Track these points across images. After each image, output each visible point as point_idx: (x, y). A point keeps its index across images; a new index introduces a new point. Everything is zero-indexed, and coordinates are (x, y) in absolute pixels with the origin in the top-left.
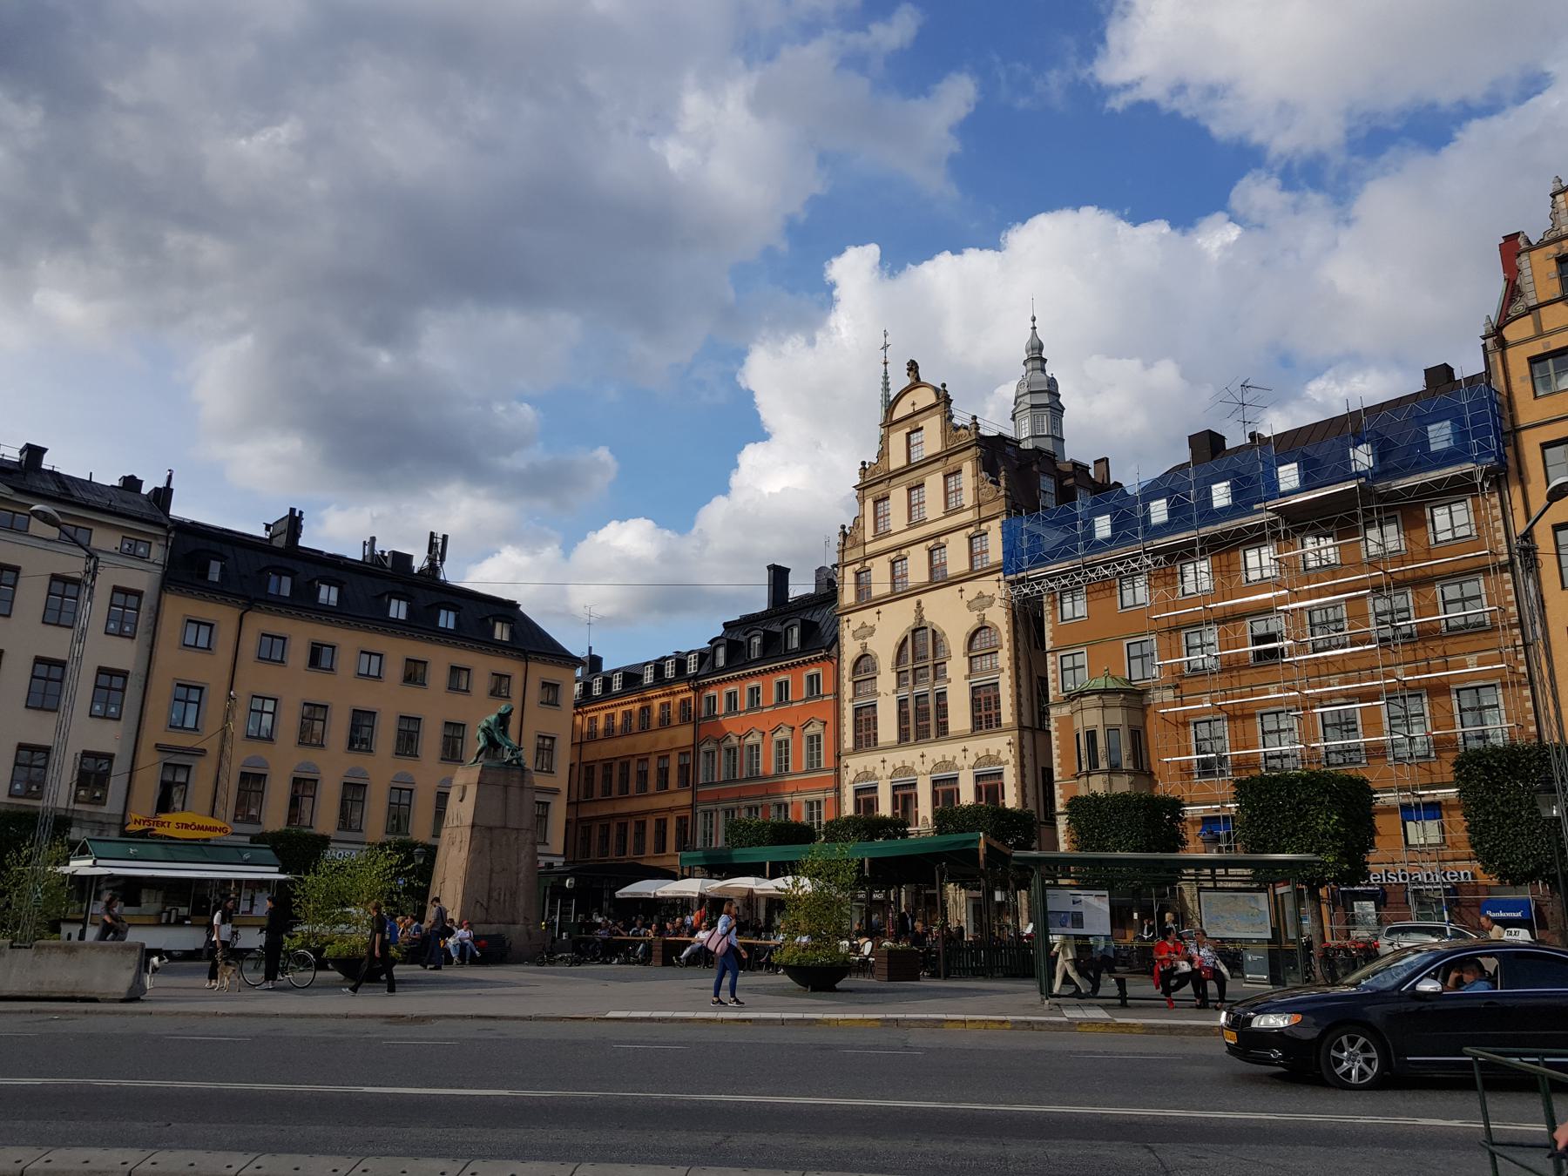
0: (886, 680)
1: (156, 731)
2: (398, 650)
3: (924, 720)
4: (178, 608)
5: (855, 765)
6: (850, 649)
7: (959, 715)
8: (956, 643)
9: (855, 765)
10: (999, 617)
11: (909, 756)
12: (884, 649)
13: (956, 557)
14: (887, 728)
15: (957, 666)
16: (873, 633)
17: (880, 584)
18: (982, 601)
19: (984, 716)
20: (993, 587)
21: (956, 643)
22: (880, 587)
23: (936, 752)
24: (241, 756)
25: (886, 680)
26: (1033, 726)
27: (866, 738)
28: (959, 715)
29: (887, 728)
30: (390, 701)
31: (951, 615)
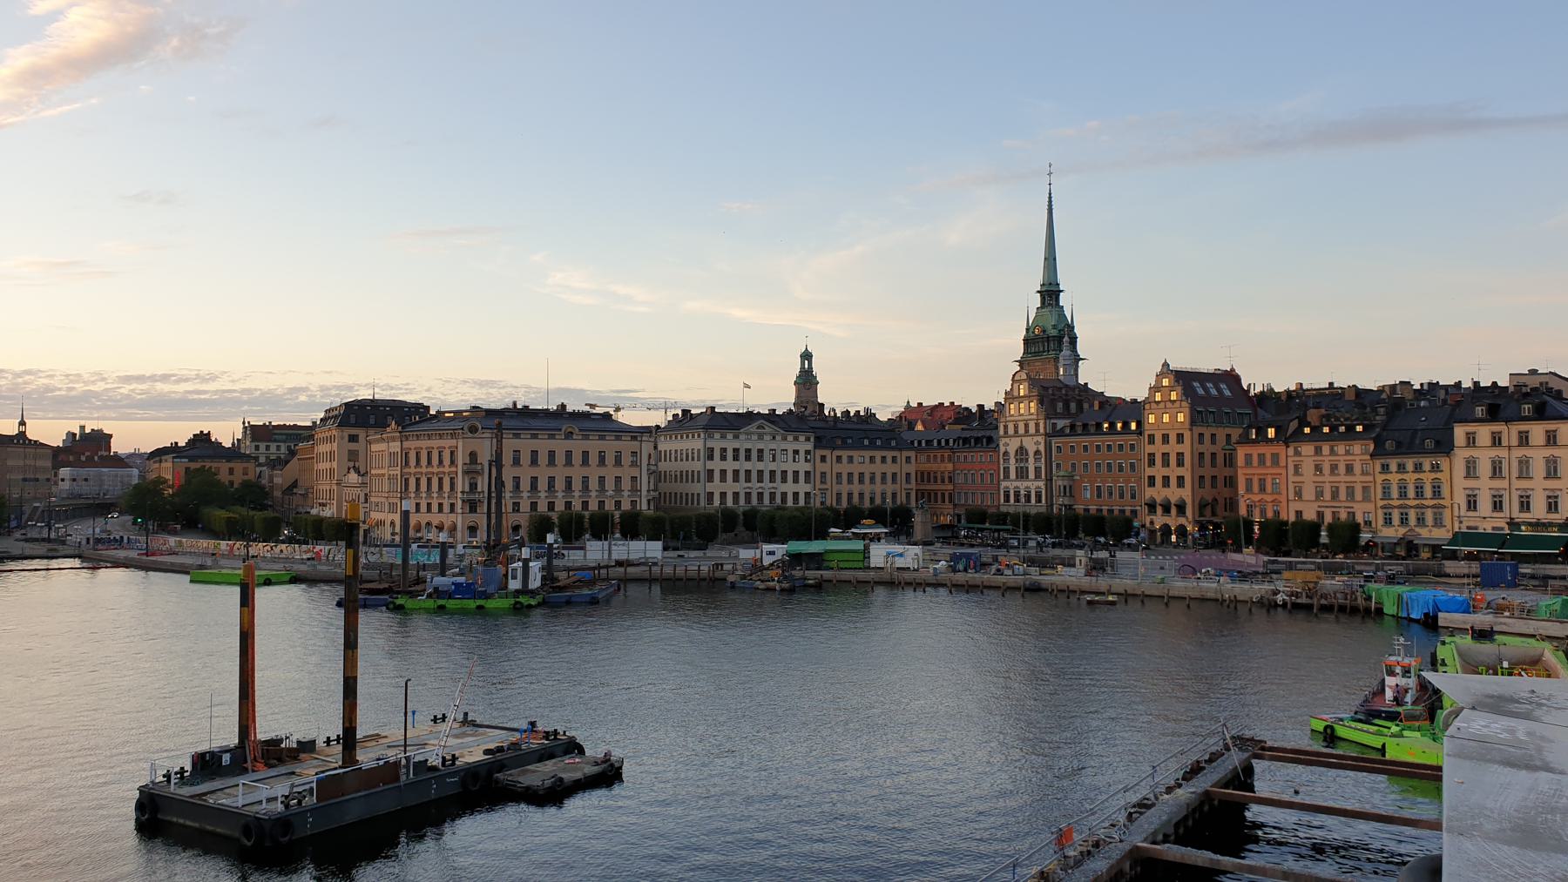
0: (1012, 461)
1: (818, 485)
2: (868, 454)
3: (1022, 474)
4: (819, 453)
5: (1004, 484)
6: (1002, 449)
7: (1032, 475)
8: (1031, 454)
9: (1004, 484)
10: (1042, 448)
11: (1018, 484)
12: (1012, 450)
13: (1032, 430)
14: (1013, 475)
15: (1031, 460)
16: (1010, 445)
17: (1011, 431)
18: (1037, 443)
19: (1038, 476)
20: (1041, 439)
21: (1031, 454)
22: (1011, 431)
23: (1026, 484)
24: (836, 488)
25: (1012, 461)
26: (1049, 480)
27: (1007, 476)
28: (1032, 475)
29: (1013, 475)
30: (867, 469)
31: (1030, 445)
